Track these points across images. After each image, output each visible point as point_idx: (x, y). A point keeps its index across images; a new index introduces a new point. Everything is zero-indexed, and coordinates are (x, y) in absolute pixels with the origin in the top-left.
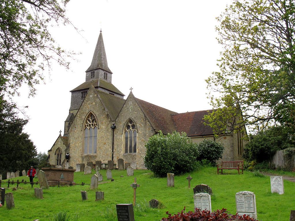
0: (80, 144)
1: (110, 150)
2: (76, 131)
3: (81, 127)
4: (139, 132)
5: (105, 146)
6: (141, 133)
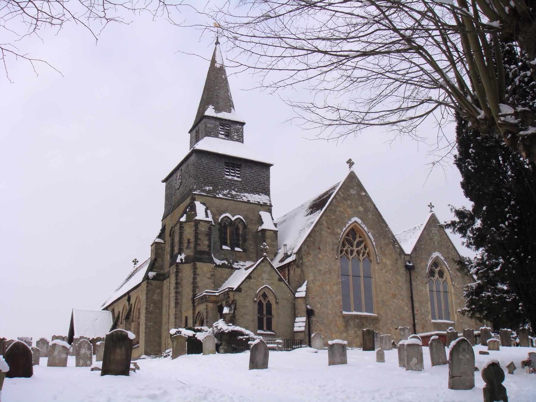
0: (335, 288)
1: (407, 309)
2: (320, 256)
3: (333, 249)
5: (395, 300)
6: (458, 287)
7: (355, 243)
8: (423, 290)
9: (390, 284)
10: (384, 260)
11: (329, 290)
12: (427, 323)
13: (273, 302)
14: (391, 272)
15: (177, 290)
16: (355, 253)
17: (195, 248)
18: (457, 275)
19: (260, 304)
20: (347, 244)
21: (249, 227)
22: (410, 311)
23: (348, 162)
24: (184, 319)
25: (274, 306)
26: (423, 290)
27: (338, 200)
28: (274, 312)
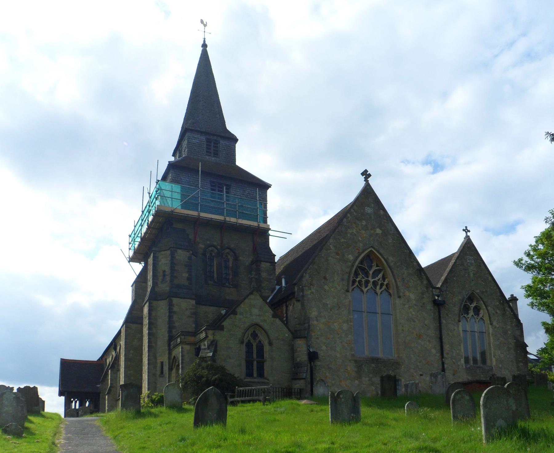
2: (326, 287)
3: (343, 280)
4: (495, 323)
5: (420, 341)
6: (497, 326)
7: (371, 272)
8: (454, 330)
9: (414, 321)
10: (407, 293)
11: (337, 328)
12: (458, 369)
13: (266, 343)
14: (416, 307)
15: (150, 331)
16: (370, 285)
17: (172, 281)
18: (497, 313)
19: (249, 346)
20: (361, 273)
21: (241, 258)
22: (438, 355)
23: (363, 174)
24: (159, 365)
25: (267, 348)
26: (454, 330)
27: (349, 219)
28: (266, 355)
